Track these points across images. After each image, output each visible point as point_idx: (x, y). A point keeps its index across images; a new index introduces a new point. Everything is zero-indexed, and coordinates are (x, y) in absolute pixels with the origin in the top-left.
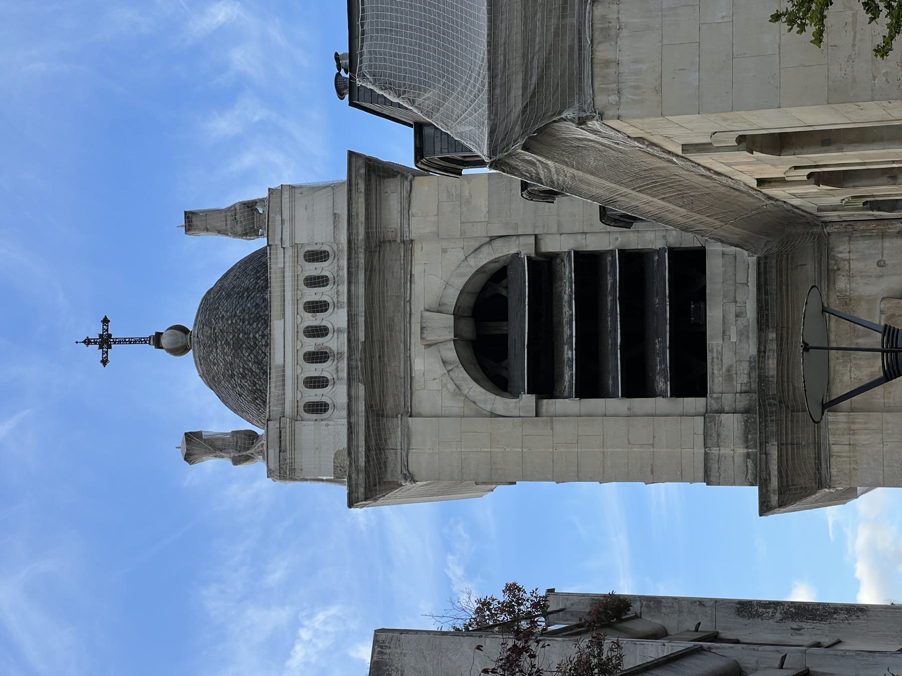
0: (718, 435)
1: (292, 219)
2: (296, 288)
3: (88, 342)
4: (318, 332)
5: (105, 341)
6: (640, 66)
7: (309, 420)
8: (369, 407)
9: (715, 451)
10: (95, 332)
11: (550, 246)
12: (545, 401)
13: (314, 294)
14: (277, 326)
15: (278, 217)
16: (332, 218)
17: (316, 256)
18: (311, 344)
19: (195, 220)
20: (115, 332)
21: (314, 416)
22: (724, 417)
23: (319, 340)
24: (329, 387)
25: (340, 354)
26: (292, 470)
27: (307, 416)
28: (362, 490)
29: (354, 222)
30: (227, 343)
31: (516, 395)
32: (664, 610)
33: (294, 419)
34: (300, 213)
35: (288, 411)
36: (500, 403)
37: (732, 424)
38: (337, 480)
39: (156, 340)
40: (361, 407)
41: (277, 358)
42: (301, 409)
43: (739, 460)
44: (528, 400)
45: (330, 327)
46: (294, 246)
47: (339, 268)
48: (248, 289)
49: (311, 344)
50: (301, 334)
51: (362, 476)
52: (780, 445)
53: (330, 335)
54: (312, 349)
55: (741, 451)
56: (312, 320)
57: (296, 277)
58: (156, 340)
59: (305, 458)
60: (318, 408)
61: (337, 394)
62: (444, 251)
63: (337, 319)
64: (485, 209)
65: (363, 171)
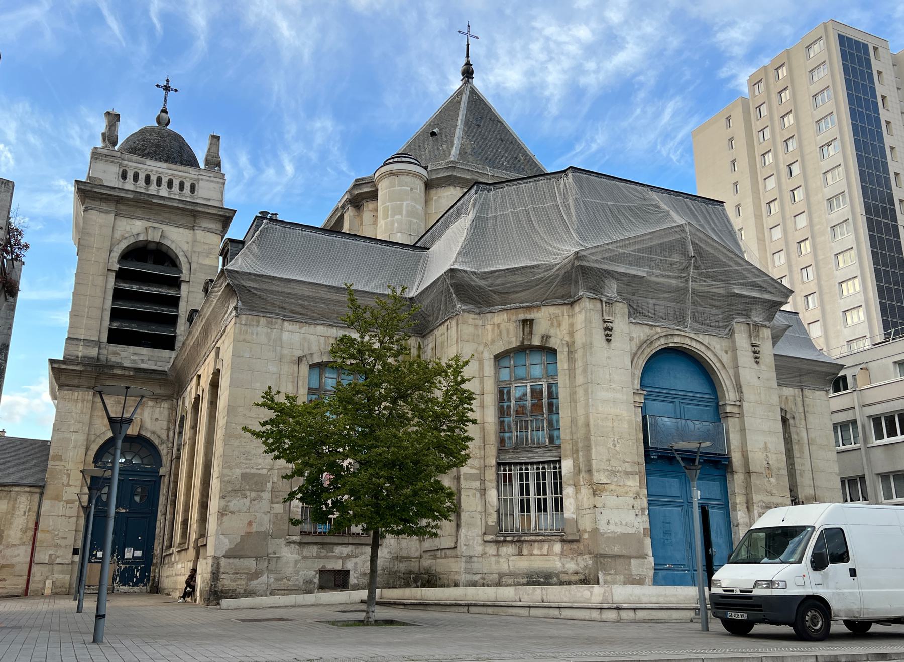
0: (88, 346)
1: (210, 181)
2: (180, 177)
3: (168, 81)
4: (159, 182)
5: (167, 88)
6: (255, 334)
7: (119, 170)
8: (122, 198)
9: (82, 343)
11: (184, 288)
12: (114, 274)
13: (176, 183)
14: (164, 165)
15: (212, 175)
16: (208, 198)
17: (193, 188)
18: (154, 178)
19: (215, 140)
20: (171, 93)
21: (120, 173)
22: (97, 349)
23: (155, 182)
24: (133, 182)
25: (147, 190)
26: (96, 159)
27: (121, 170)
28: (83, 187)
29: (206, 207)
30: (159, 142)
31: (119, 262)
32: (8, 312)
33: (120, 164)
34: (212, 185)
35: (124, 162)
36: (116, 255)
37: (93, 352)
38: (89, 177)
39: (164, 111)
40: (122, 195)
41: (149, 162)
42: (124, 168)
43: (76, 353)
44: (116, 267)
45: (160, 188)
46: (199, 180)
47: (186, 197)
48: (182, 156)
50: (159, 175)
51: (89, 189)
52: (80, 371)
53: (157, 187)
54: (151, 178)
55: (80, 354)
56: (165, 180)
57: (185, 178)
58: (164, 111)
60: (124, 175)
61: (129, 185)
62: (188, 243)
63: (164, 192)
64: (203, 262)
65: (227, 215)
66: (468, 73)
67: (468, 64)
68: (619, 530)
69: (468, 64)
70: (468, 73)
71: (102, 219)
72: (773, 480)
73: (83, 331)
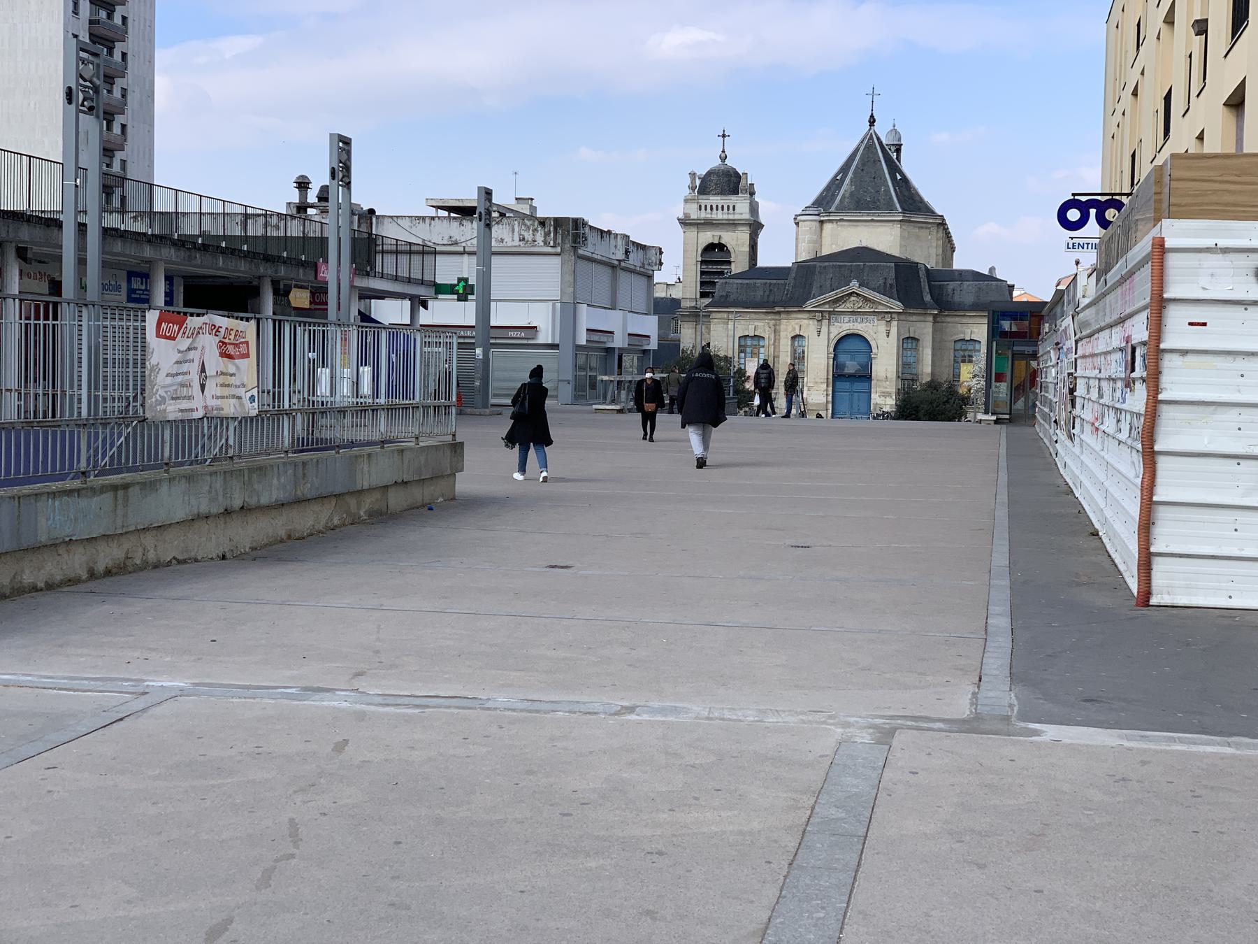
5: (724, 136)
10: (726, 133)
11: (733, 264)
13: (725, 208)
14: (719, 198)
17: (734, 207)
18: (714, 207)
20: (726, 139)
25: (711, 214)
31: (701, 256)
33: (698, 203)
37: (693, 304)
38: (684, 214)
39: (723, 152)
44: (700, 259)
49: (714, 207)
58: (723, 152)
59: (688, 205)
61: (703, 215)
66: (872, 121)
67: (872, 116)
68: (816, 402)
69: (872, 116)
70: (872, 121)
71: (692, 233)
72: (888, 383)
73: (688, 294)
